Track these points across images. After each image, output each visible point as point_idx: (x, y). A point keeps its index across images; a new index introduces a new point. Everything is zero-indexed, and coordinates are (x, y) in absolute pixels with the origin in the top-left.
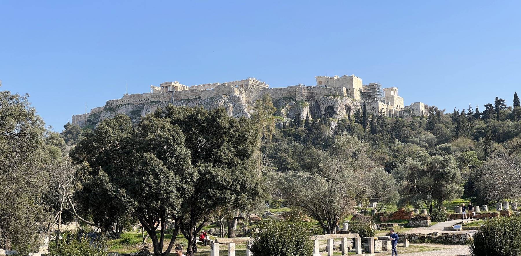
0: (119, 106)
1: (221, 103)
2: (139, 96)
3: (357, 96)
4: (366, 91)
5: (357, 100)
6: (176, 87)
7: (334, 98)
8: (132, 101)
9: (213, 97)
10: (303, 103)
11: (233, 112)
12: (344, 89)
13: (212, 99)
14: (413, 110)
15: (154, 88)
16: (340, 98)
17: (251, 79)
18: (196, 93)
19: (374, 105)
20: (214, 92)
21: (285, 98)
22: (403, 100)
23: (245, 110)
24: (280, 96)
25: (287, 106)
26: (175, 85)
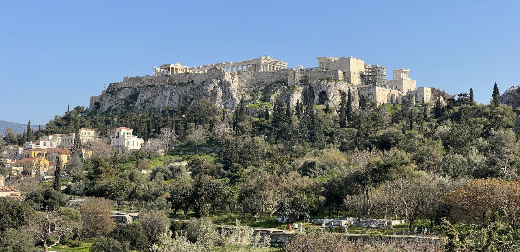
0: (120, 90)
1: (211, 88)
2: (138, 79)
3: (356, 80)
4: (367, 74)
5: (355, 84)
6: (176, 69)
7: (328, 83)
8: (131, 84)
9: (205, 82)
10: (294, 88)
11: (222, 97)
12: (340, 73)
13: (203, 83)
14: (416, 96)
15: (156, 69)
16: (333, 83)
17: (263, 58)
18: (190, 77)
19: (371, 90)
20: (207, 76)
21: (278, 82)
22: (415, 82)
23: (235, 96)
24: (273, 80)
25: (278, 91)
26: (175, 67)
